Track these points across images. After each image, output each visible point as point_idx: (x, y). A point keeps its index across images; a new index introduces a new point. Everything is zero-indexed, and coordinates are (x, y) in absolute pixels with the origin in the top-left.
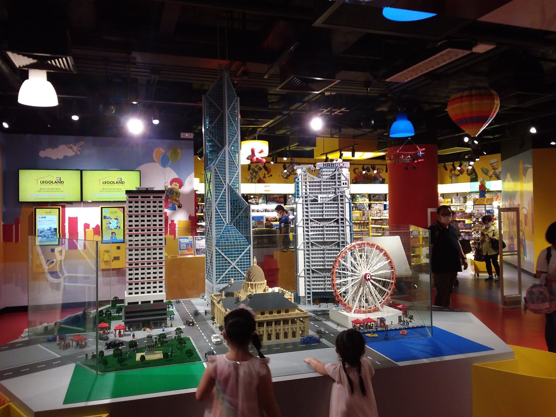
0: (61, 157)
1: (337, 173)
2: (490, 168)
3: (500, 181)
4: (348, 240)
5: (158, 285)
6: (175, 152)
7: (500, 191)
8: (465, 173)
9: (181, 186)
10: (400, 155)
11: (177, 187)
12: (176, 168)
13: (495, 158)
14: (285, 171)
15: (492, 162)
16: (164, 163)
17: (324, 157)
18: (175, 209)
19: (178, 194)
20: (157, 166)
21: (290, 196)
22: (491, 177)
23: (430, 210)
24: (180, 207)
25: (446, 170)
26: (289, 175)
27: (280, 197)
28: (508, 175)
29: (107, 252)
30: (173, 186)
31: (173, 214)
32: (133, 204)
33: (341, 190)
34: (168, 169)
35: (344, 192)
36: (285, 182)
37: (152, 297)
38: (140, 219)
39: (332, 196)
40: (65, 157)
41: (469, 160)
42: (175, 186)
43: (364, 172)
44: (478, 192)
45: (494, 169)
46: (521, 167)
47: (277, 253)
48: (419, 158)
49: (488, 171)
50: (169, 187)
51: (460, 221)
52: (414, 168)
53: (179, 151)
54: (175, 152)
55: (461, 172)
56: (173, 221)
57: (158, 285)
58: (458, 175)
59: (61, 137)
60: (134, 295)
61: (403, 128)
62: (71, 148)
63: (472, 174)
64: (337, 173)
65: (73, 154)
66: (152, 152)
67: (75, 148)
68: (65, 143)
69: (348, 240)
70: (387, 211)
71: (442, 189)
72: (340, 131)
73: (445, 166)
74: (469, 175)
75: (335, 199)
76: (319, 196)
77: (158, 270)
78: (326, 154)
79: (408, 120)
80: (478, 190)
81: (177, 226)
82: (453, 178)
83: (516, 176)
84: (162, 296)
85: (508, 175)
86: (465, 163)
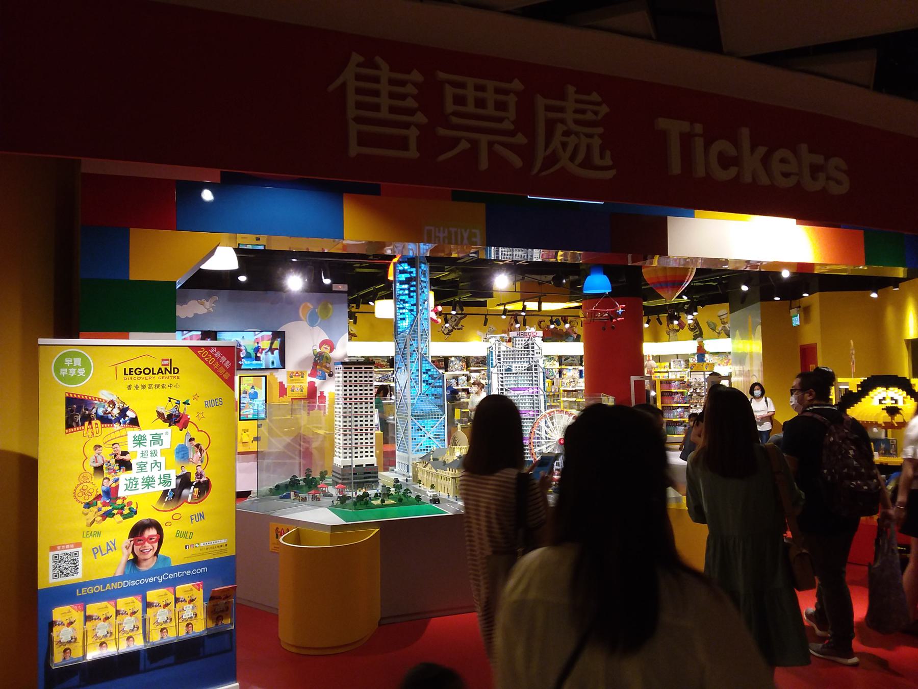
0: (191, 316)
1: (530, 342)
2: (718, 322)
3: (730, 339)
4: (542, 409)
5: (369, 450)
6: (326, 309)
7: (730, 353)
8: (686, 328)
9: (331, 351)
10: (596, 312)
11: (327, 351)
12: (326, 329)
13: (723, 309)
14: (447, 325)
15: (721, 313)
16: (312, 323)
17: (502, 308)
18: (325, 378)
19: (328, 359)
20: (304, 325)
21: (453, 359)
22: (719, 333)
23: (633, 378)
24: (331, 375)
25: (661, 324)
26: (452, 331)
27: (439, 361)
28: (737, 332)
29: (246, 431)
30: (323, 350)
31: (322, 384)
32: (348, 375)
33: (535, 359)
34: (317, 329)
35: (538, 361)
36: (446, 340)
37: (364, 461)
38: (353, 388)
39: (526, 365)
40: (196, 315)
41: (689, 312)
42: (325, 349)
43: (552, 327)
44: (694, 354)
45: (723, 323)
46: (750, 319)
47: (452, 428)
48: (618, 316)
49: (715, 325)
50: (318, 350)
51: (677, 393)
52: (613, 328)
53: (330, 306)
54: (326, 309)
55: (681, 325)
56: (322, 393)
57: (369, 450)
58: (678, 331)
59: (191, 290)
60: (348, 459)
61: (598, 283)
62: (202, 304)
63: (695, 329)
64: (530, 342)
65: (205, 311)
66: (298, 309)
67: (208, 304)
68: (197, 298)
69: (542, 409)
70: (583, 379)
71: (649, 349)
72: (523, 278)
73: (658, 319)
74: (692, 330)
75: (528, 369)
76: (514, 365)
77: (369, 436)
78: (505, 305)
79: (604, 274)
80: (695, 351)
81: (327, 399)
82: (671, 334)
83: (745, 336)
84: (373, 461)
85: (737, 332)
86: (683, 316)
